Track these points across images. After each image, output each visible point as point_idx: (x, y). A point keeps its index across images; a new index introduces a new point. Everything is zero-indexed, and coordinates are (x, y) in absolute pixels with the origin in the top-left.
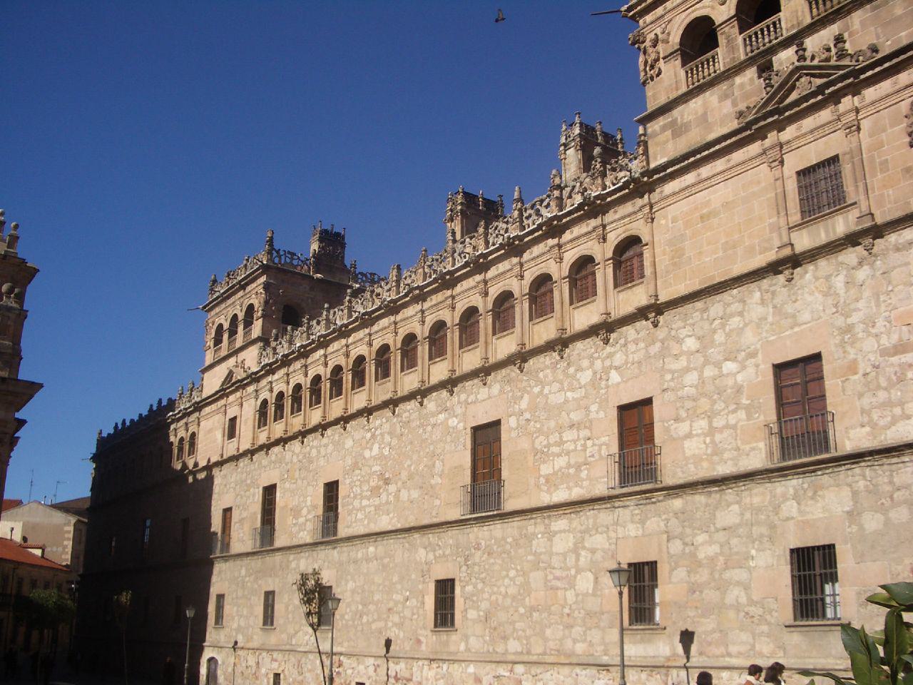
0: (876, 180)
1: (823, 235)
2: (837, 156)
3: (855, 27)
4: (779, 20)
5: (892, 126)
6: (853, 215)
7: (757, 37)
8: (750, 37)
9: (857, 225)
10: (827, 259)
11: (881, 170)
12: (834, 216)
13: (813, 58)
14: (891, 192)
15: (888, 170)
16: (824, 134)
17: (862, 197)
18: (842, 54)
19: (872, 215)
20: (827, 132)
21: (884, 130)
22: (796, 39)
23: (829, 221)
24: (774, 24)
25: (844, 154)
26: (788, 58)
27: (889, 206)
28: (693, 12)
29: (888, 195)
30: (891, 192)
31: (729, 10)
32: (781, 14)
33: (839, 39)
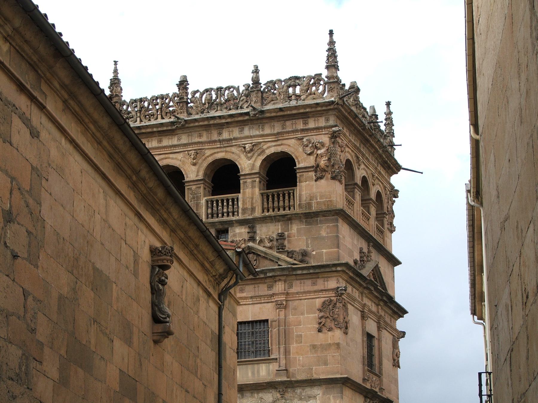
0: (294, 347)
1: (250, 374)
2: (267, 321)
3: (293, 231)
4: (238, 199)
5: (308, 313)
6: (274, 367)
7: (217, 205)
8: (212, 202)
9: (277, 375)
10: (252, 393)
11: (296, 341)
12: (259, 363)
13: (261, 241)
14: (301, 358)
15: (301, 342)
16: (260, 302)
17: (282, 356)
18: (281, 248)
19: (286, 370)
20: (263, 301)
21: (302, 314)
22: (251, 224)
23: (256, 366)
24: (233, 200)
25: (272, 321)
26: (240, 234)
27: (298, 367)
28: (166, 158)
29: (299, 360)
30: (301, 358)
31: (198, 172)
32: (240, 196)
33: (281, 236)
